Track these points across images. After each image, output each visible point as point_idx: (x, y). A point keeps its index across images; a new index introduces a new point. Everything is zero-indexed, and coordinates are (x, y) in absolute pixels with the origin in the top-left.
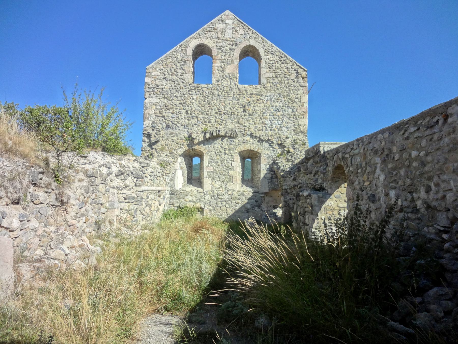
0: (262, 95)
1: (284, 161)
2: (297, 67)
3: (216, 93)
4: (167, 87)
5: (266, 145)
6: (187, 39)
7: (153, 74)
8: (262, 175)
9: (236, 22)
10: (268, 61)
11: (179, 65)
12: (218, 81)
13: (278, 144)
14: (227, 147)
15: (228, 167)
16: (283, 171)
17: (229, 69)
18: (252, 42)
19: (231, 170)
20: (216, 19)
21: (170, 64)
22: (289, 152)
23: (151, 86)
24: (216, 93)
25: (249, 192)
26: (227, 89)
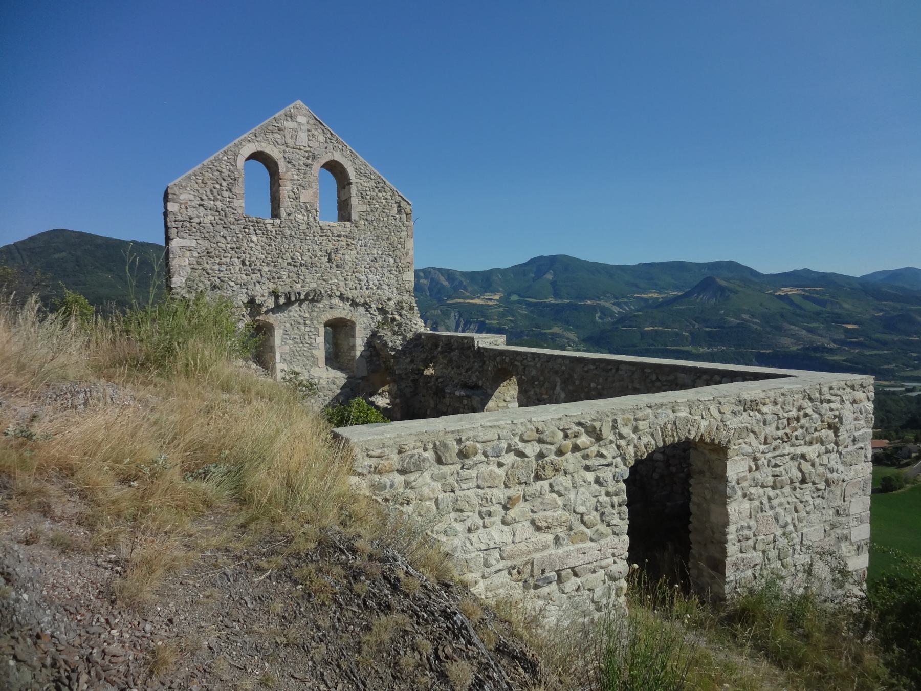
0: (353, 239)
1: (389, 334)
2: (399, 199)
3: (288, 232)
4: (207, 220)
5: (361, 310)
6: (236, 141)
7: (182, 197)
8: (358, 354)
9: (312, 122)
10: (360, 187)
11: (224, 184)
12: (289, 215)
13: (378, 308)
14: (307, 315)
15: (310, 344)
16: (393, 349)
17: (305, 196)
18: (337, 156)
19: (316, 348)
20: (282, 112)
21: (209, 182)
22: (393, 320)
23: (179, 218)
24: (288, 232)
25: (340, 378)
26: (303, 227)
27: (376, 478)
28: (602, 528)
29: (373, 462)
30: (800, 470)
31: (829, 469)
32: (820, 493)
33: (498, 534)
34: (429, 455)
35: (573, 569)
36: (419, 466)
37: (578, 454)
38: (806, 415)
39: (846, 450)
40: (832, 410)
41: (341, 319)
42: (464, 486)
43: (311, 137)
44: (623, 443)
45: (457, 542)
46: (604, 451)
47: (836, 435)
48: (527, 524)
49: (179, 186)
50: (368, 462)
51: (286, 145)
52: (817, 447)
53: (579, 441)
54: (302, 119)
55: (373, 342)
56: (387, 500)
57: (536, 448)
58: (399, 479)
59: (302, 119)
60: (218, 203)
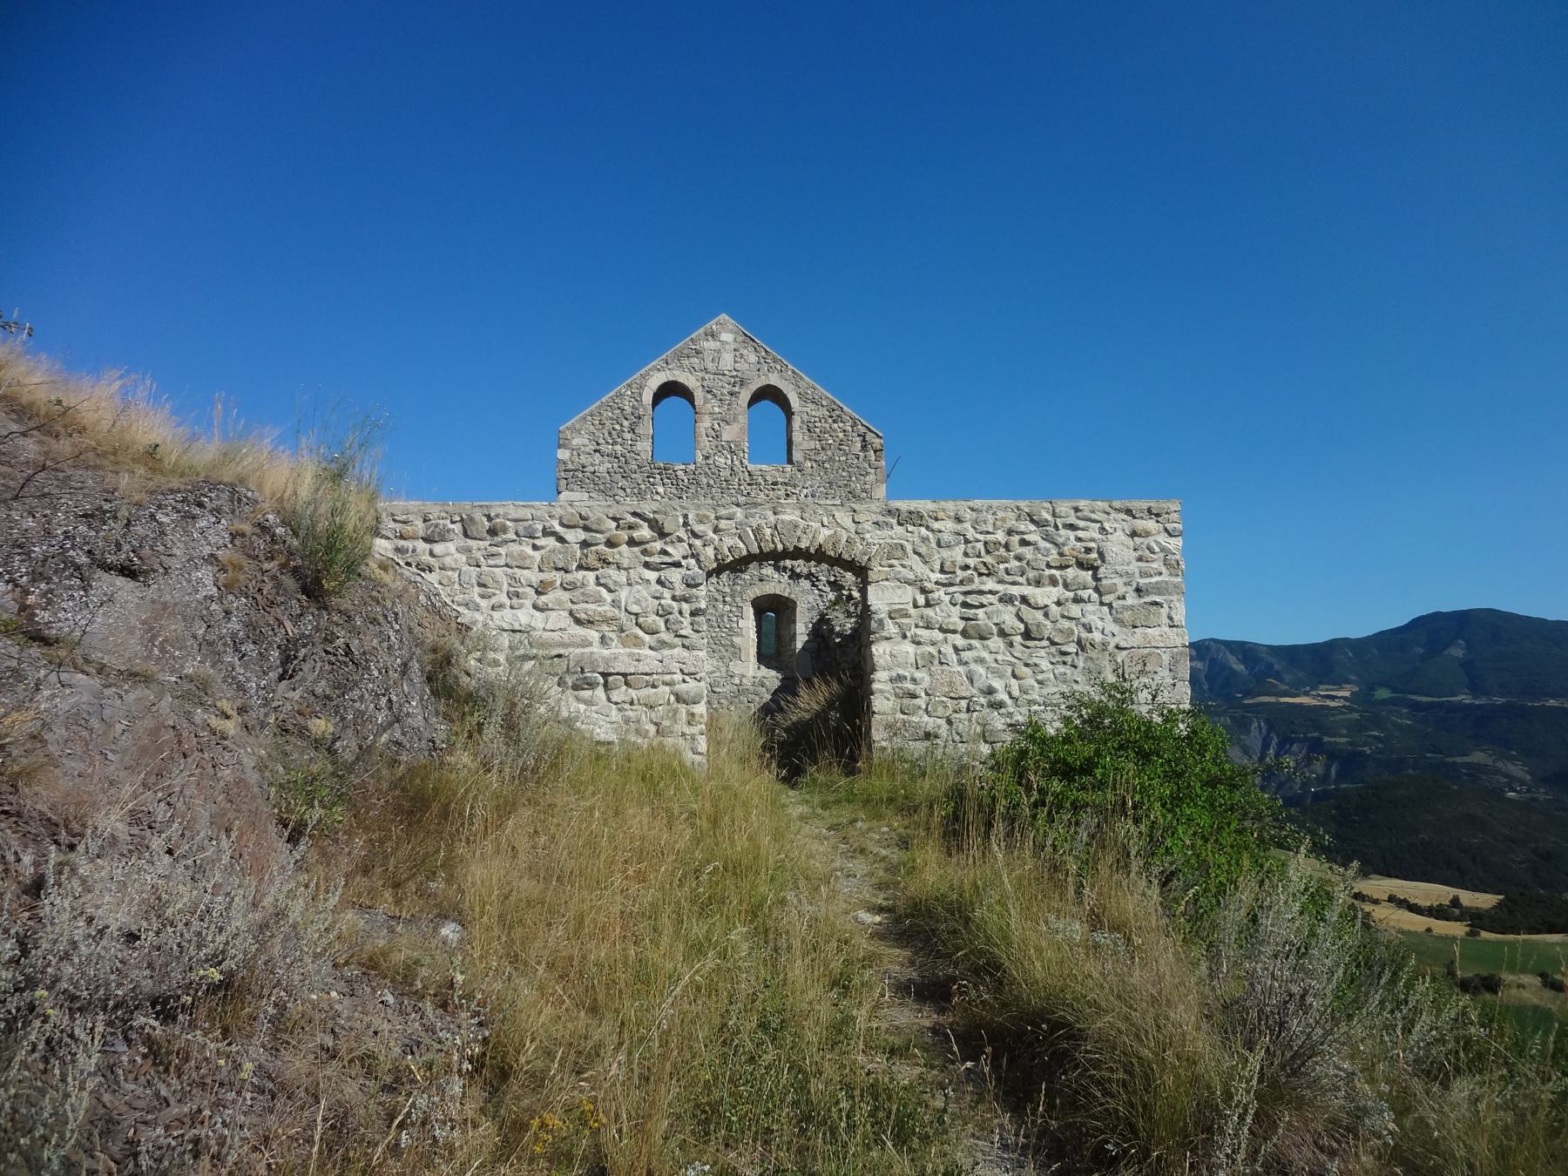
0: (795, 486)
1: (841, 616)
2: (863, 430)
3: (705, 480)
4: (603, 469)
5: (806, 584)
6: (642, 371)
7: (574, 442)
8: (799, 645)
9: (740, 339)
10: (806, 418)
11: (626, 423)
12: (707, 458)
13: (829, 582)
14: (727, 589)
15: (731, 629)
16: (839, 635)
17: (728, 434)
18: (774, 380)
19: (738, 635)
20: (701, 331)
21: (608, 423)
22: (850, 597)
23: (570, 466)
24: (705, 480)
25: (772, 678)
26: (725, 473)
27: (402, 543)
28: (665, 636)
29: (398, 526)
30: (1021, 620)
31: (1084, 625)
32: (1068, 659)
33: (525, 616)
34: (457, 528)
35: (624, 675)
36: (443, 537)
37: (636, 549)
38: (1024, 543)
39: (1121, 602)
40: (1079, 539)
41: (775, 595)
42: (491, 562)
43: (738, 356)
44: (698, 543)
45: (479, 617)
46: (669, 549)
47: (1096, 578)
48: (566, 614)
49: (573, 429)
50: (392, 525)
51: (706, 370)
52: (1057, 592)
53: (636, 534)
54: (726, 337)
55: (821, 629)
56: (408, 564)
57: (582, 535)
58: (422, 546)
59: (726, 337)
60: (618, 448)
